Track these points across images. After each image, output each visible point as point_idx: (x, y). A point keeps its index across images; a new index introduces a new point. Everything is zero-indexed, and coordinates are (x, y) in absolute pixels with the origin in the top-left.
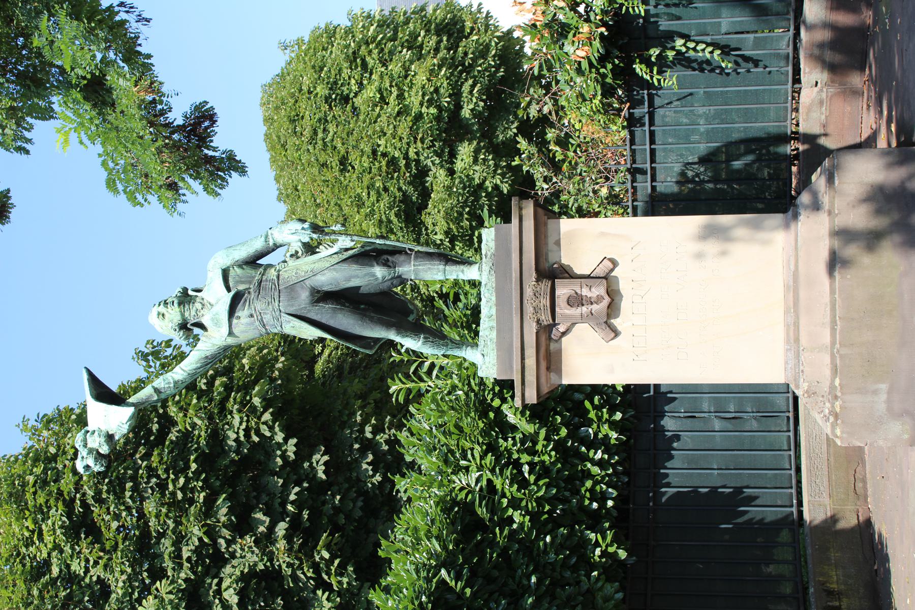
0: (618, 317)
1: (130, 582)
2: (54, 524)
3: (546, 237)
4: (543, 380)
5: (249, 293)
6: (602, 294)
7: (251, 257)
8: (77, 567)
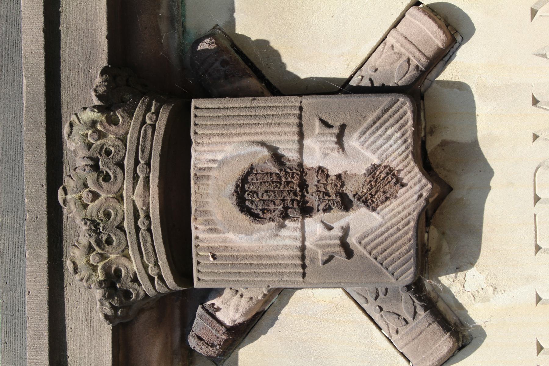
0: (471, 264)
6: (395, 163)
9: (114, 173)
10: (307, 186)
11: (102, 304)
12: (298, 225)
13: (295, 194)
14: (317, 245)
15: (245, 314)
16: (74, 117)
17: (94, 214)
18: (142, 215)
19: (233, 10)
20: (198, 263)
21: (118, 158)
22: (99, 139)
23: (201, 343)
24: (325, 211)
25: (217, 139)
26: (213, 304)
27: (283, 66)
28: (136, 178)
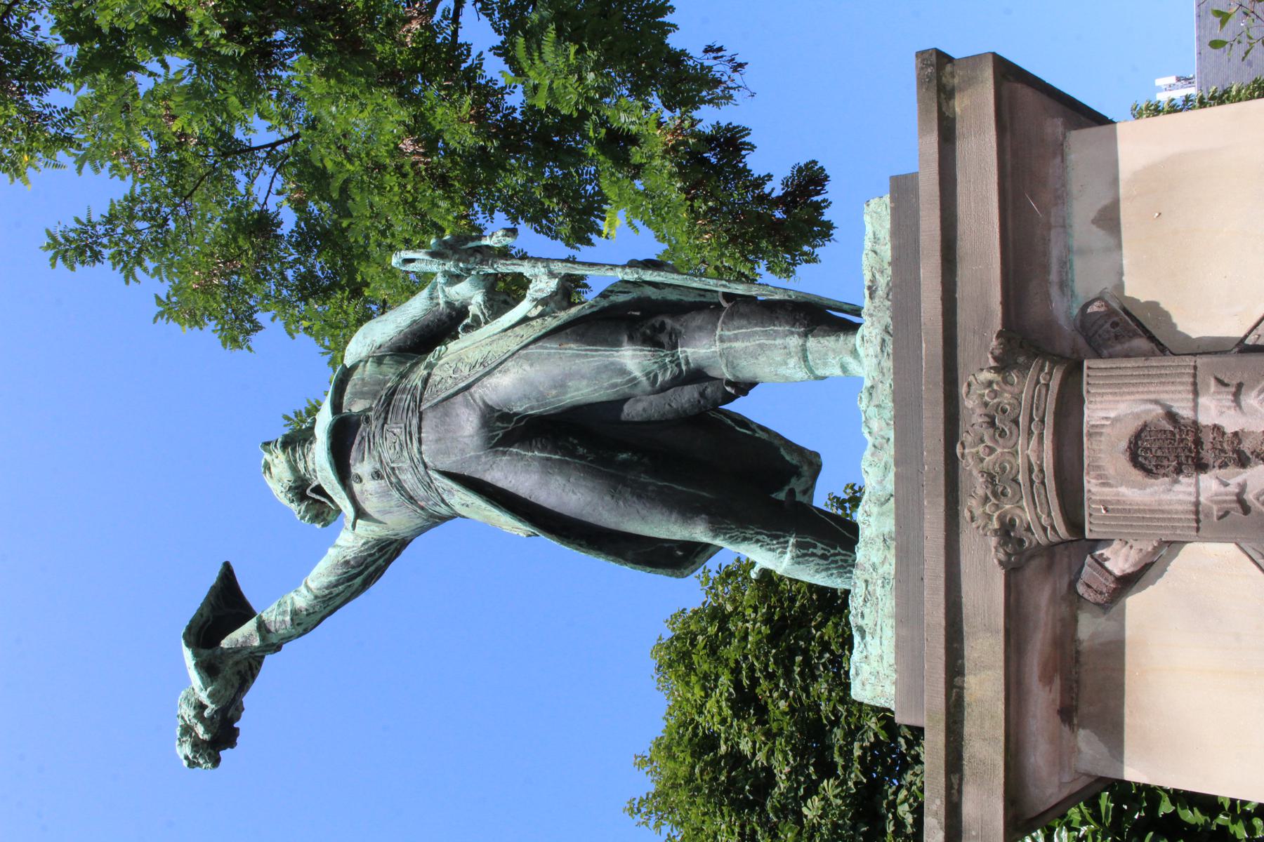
1: (797, 776)
2: (721, 695)
3: (1061, 197)
4: (1038, 757)
5: (368, 419)
7: (406, 335)
8: (745, 746)
9: (1010, 429)
10: (1202, 443)
11: (997, 550)
12: (1192, 480)
13: (1190, 451)
14: (1212, 501)
15: (1134, 565)
16: (971, 378)
17: (991, 467)
18: (1036, 469)
19: (1121, 274)
20: (1090, 515)
21: (1013, 416)
22: (995, 397)
23: (1090, 590)
24: (1220, 467)
25: (1110, 398)
26: (1102, 554)
27: (1174, 326)
28: (1030, 433)
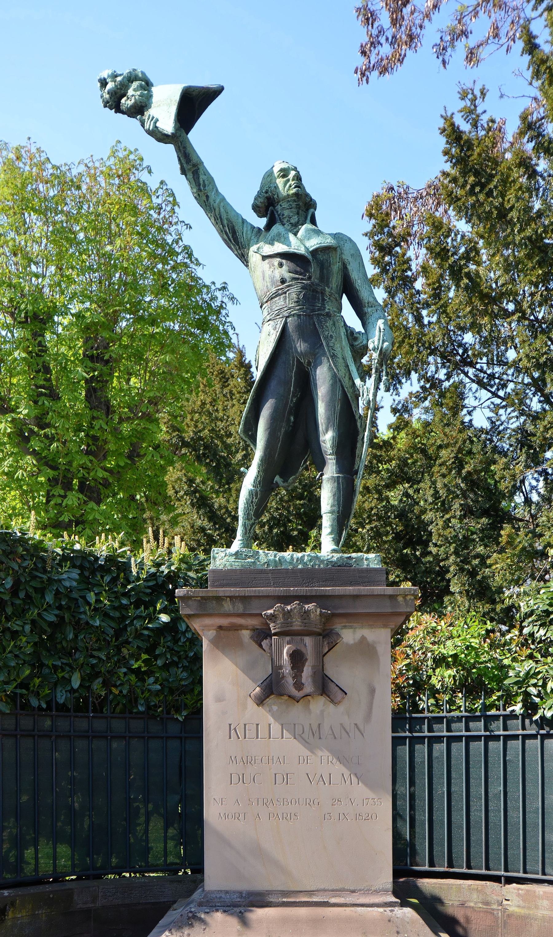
3: (371, 626)
